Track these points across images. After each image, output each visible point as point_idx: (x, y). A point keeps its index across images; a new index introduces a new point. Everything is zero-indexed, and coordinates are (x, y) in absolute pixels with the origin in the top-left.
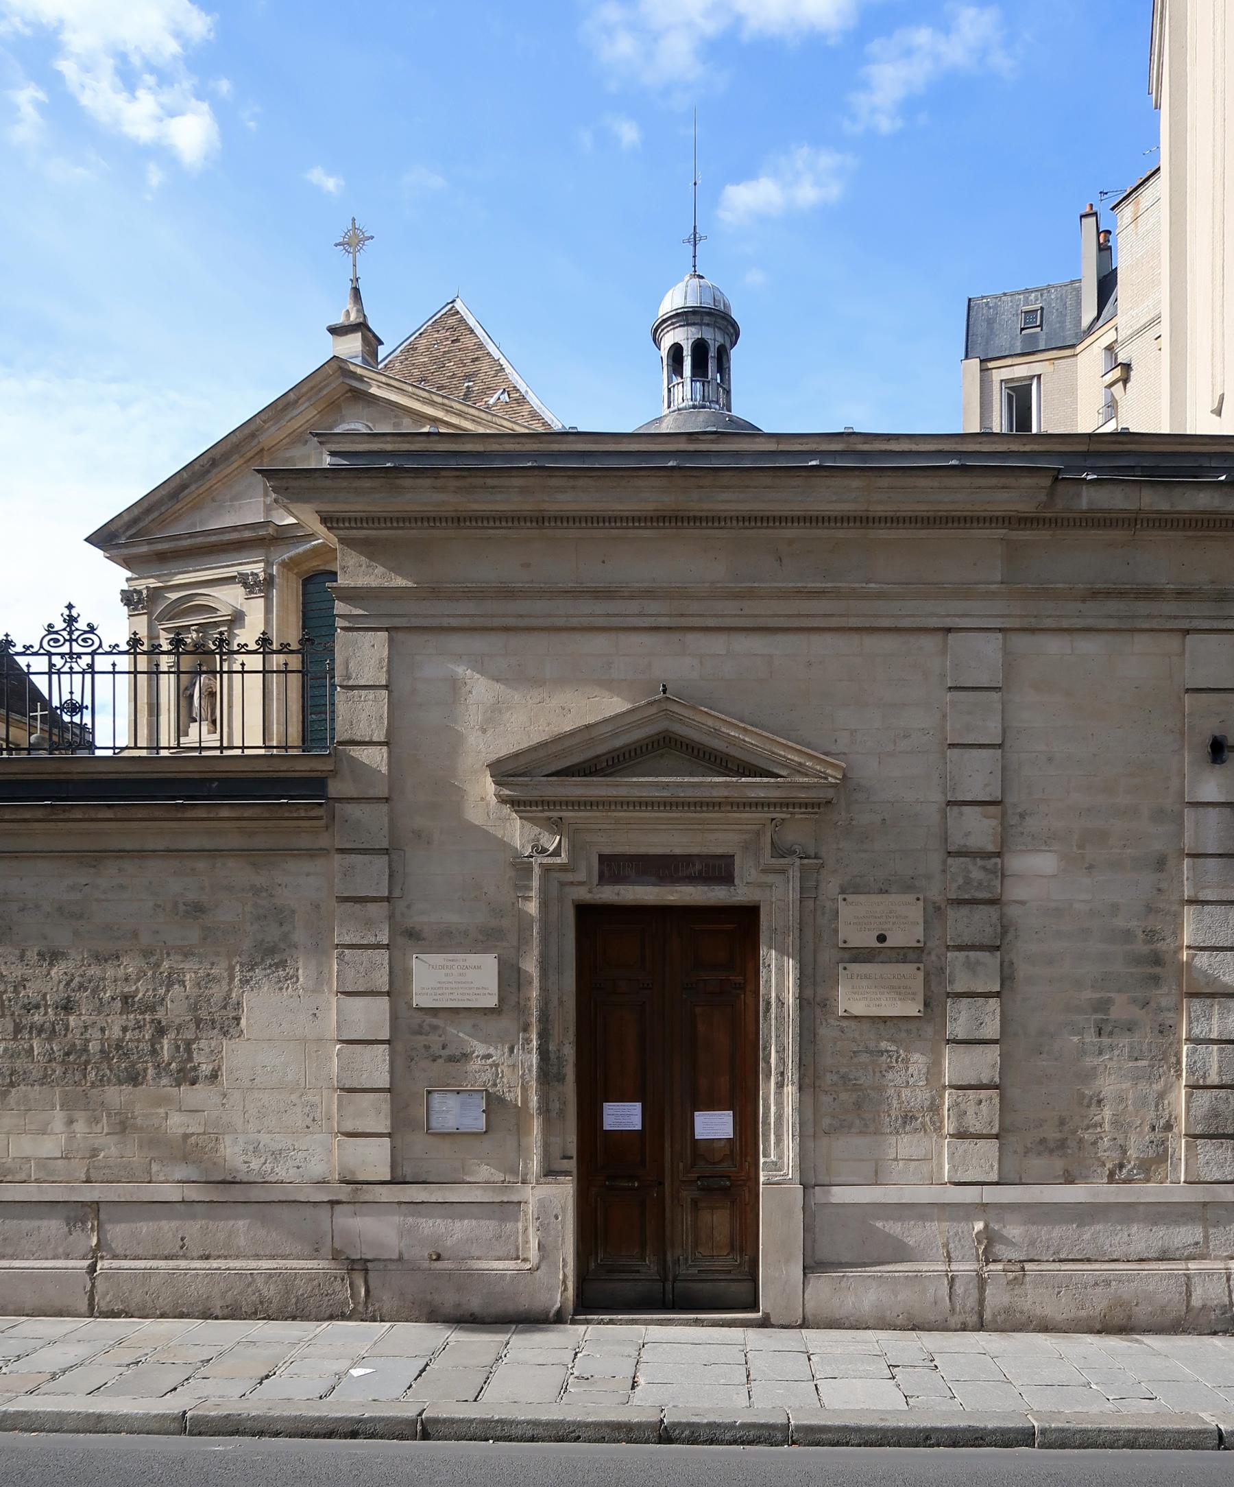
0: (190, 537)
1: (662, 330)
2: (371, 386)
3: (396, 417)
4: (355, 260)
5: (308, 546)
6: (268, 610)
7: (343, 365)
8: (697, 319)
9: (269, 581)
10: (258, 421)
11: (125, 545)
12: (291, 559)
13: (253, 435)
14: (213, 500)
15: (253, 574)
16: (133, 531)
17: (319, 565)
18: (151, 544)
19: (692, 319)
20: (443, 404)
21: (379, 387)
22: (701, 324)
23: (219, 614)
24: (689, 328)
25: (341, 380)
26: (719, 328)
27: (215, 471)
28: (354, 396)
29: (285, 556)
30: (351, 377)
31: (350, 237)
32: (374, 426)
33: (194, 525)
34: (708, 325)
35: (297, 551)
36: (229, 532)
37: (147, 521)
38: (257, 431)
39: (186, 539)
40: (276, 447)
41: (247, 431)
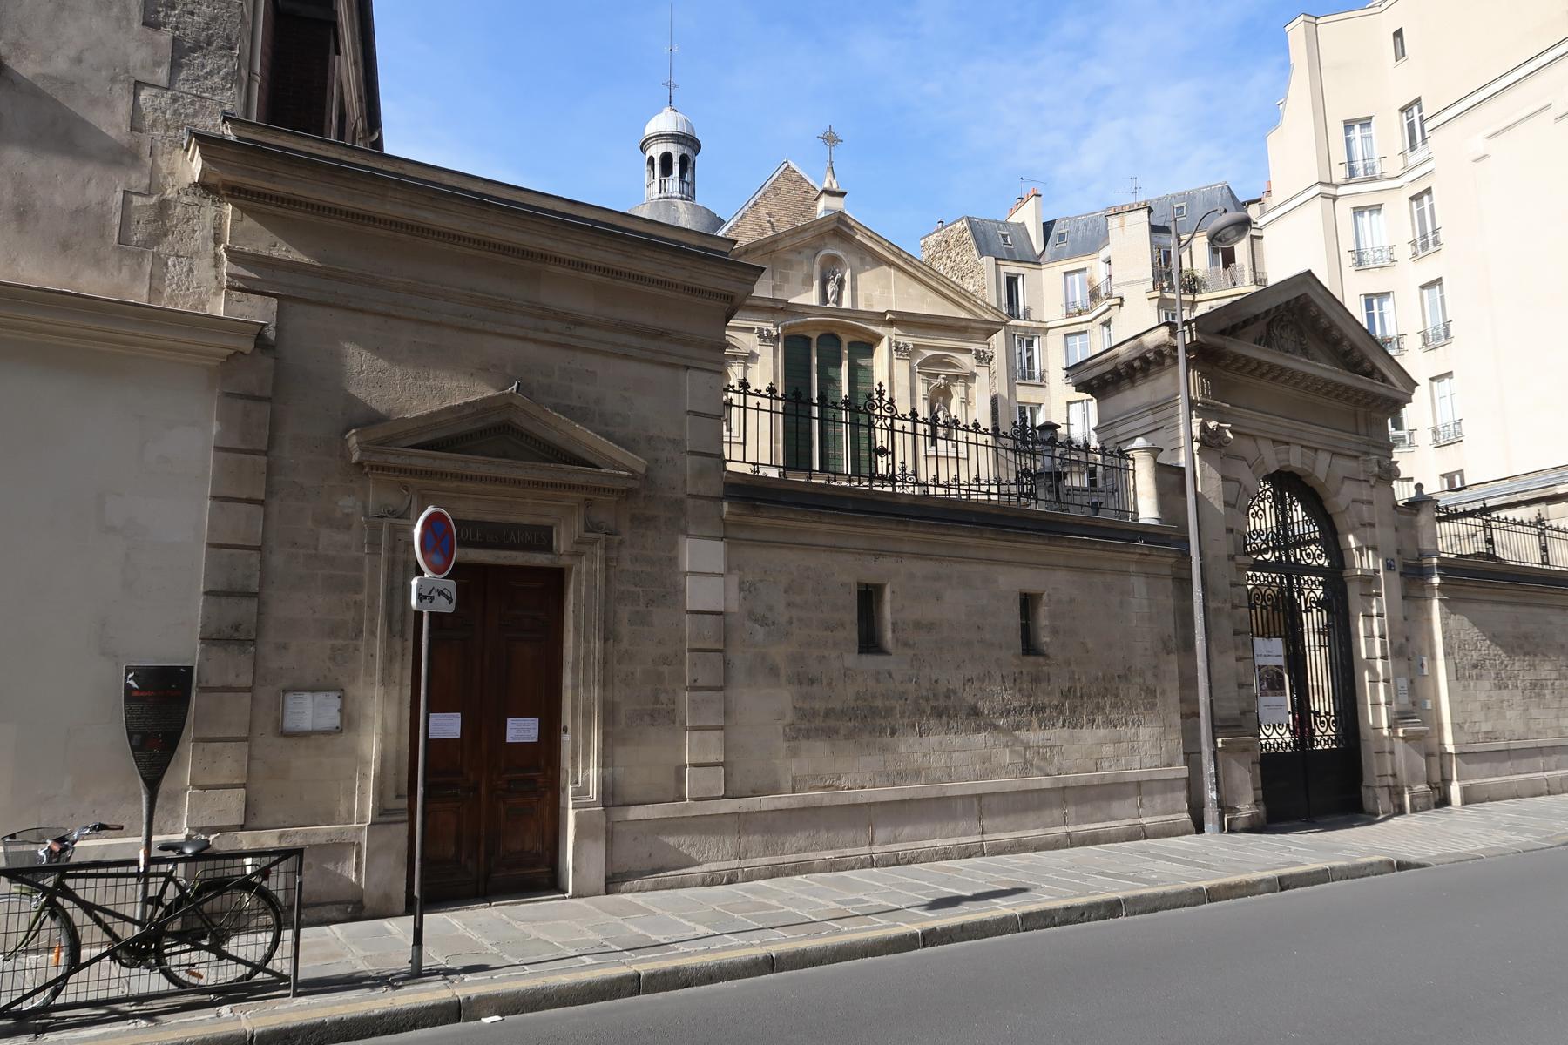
3: (861, 254)
5: (804, 320)
6: (775, 355)
9: (778, 335)
12: (790, 325)
13: (775, 242)
15: (767, 330)
19: (681, 140)
21: (862, 236)
22: (685, 145)
23: (739, 351)
25: (836, 224)
28: (834, 233)
30: (842, 224)
34: (689, 146)
41: (774, 239)
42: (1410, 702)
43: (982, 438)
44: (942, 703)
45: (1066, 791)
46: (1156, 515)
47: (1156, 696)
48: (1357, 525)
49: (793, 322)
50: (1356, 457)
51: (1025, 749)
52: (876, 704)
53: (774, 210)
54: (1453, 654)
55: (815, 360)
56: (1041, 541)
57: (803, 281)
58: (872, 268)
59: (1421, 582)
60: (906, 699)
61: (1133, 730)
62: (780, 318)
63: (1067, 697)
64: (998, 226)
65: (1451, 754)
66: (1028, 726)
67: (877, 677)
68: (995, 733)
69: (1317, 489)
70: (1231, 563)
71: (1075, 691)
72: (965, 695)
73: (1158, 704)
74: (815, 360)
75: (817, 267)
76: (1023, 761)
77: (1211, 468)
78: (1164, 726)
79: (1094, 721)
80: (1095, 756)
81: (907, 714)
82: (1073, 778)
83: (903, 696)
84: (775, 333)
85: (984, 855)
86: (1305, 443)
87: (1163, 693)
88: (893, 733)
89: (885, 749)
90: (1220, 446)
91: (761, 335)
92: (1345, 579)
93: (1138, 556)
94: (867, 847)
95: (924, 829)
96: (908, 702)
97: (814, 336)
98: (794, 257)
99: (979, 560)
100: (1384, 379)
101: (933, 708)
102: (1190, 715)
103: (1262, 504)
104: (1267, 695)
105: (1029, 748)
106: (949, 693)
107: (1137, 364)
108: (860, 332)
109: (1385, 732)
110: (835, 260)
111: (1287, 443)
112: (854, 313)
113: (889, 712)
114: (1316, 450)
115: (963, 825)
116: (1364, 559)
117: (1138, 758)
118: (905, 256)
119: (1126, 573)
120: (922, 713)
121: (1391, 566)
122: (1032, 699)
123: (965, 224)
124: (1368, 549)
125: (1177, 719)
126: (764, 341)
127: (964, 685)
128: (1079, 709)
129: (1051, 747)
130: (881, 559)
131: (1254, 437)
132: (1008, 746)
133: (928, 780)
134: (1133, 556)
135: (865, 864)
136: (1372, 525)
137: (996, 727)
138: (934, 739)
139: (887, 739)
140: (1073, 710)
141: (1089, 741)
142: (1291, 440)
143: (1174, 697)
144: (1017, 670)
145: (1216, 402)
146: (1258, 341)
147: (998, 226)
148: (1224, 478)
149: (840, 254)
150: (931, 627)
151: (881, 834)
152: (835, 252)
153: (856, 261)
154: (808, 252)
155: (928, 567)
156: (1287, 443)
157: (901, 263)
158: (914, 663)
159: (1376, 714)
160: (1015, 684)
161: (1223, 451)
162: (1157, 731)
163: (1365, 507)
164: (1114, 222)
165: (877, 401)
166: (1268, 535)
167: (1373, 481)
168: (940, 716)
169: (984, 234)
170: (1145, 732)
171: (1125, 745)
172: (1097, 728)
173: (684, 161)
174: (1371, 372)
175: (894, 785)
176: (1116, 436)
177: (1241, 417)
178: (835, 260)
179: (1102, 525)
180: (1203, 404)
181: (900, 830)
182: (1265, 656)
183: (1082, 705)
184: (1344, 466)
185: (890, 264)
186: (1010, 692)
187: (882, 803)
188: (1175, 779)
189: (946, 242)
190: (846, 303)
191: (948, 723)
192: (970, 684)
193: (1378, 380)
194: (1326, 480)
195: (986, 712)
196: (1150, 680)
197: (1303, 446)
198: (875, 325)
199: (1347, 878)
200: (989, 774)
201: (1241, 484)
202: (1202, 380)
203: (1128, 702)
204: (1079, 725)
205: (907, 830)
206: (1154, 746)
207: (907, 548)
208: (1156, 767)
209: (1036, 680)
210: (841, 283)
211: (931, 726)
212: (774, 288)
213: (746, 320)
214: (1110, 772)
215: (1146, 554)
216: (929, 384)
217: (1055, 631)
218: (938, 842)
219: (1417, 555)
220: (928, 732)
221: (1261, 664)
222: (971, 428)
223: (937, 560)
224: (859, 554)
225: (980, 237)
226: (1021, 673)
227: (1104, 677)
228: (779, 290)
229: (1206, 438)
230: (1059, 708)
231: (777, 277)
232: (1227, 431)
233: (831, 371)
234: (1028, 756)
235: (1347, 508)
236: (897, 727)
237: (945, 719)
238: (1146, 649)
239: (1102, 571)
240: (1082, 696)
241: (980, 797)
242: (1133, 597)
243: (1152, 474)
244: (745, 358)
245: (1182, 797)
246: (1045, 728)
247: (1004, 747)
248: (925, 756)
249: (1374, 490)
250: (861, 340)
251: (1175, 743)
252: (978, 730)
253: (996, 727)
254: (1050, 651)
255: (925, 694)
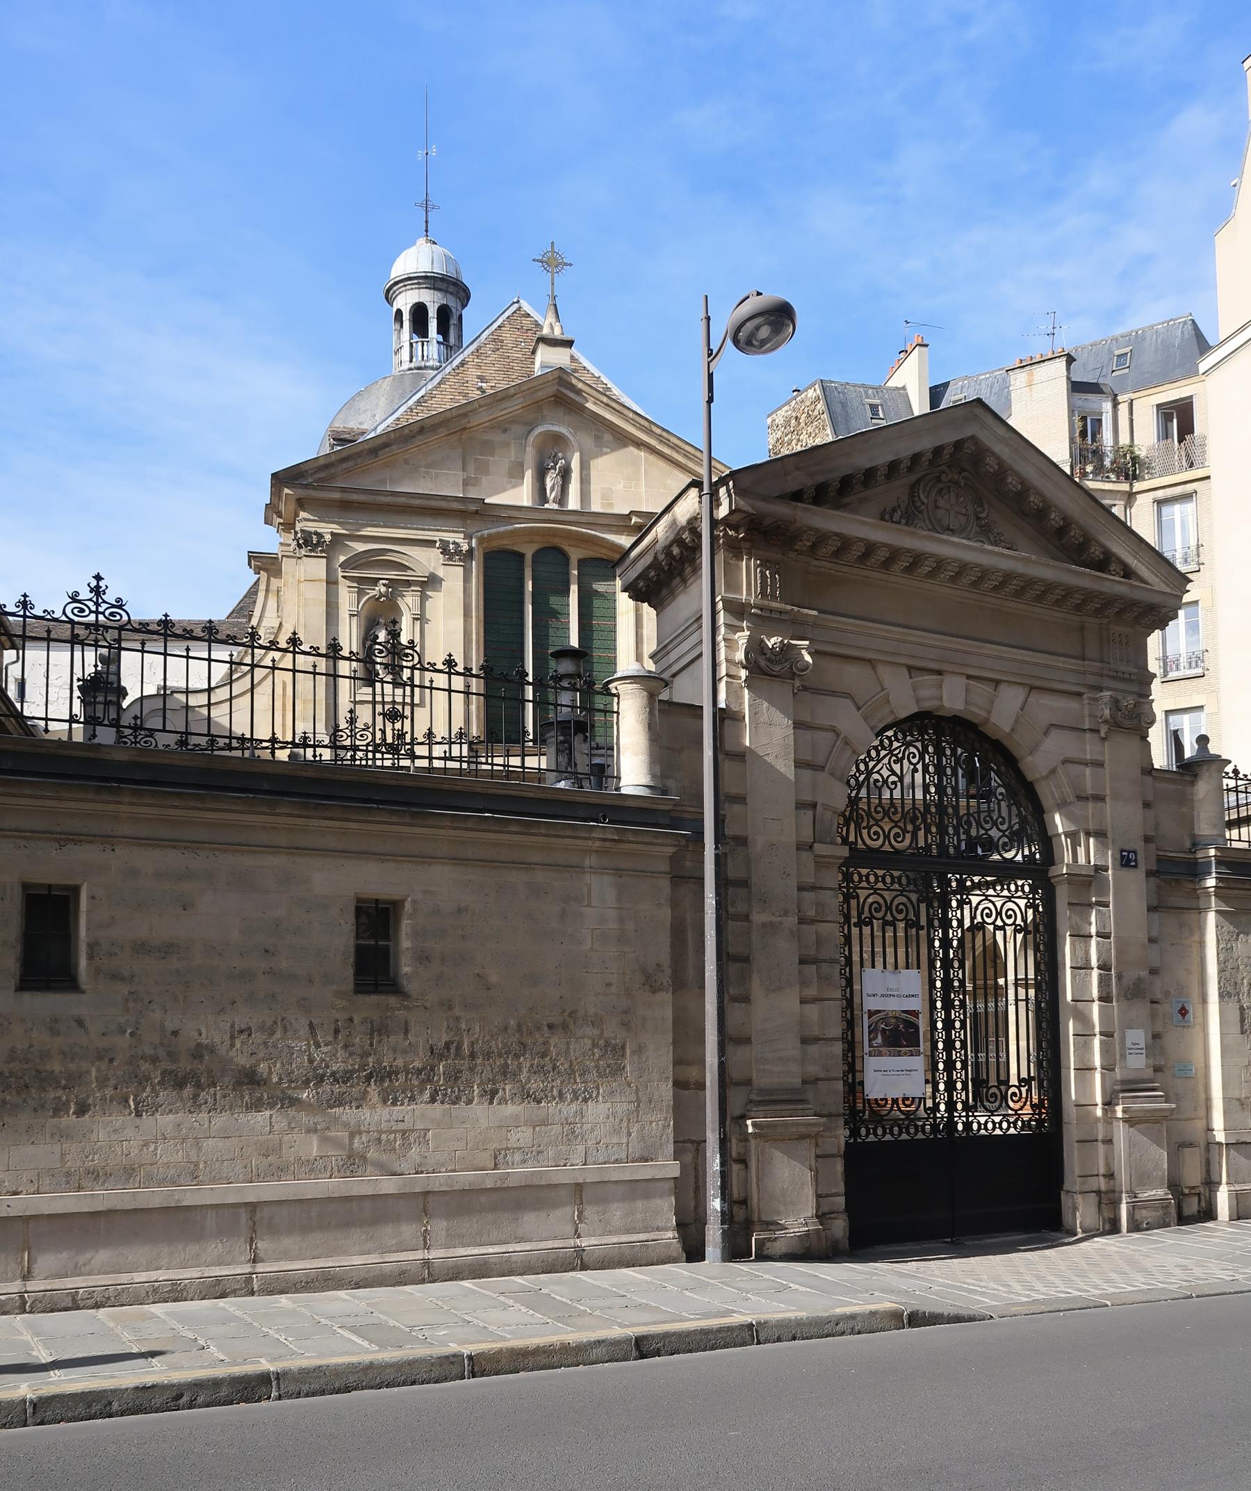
0: (391, 495)
1: (405, 286)
2: (587, 401)
3: (597, 430)
4: (553, 280)
5: (510, 527)
6: (467, 580)
7: (565, 377)
8: (444, 286)
9: (471, 551)
10: (476, 403)
11: (306, 486)
12: (490, 535)
13: (465, 415)
14: (406, 462)
15: (454, 543)
16: (322, 475)
17: (507, 545)
18: (346, 492)
19: (439, 284)
20: (660, 436)
21: (595, 403)
22: (446, 291)
23: (413, 573)
24: (436, 292)
25: (556, 387)
26: (459, 298)
27: (419, 437)
29: (486, 532)
30: (567, 388)
31: (549, 258)
32: (575, 433)
33: (383, 482)
34: (451, 293)
35: (498, 530)
36: (436, 500)
37: (339, 468)
38: (471, 412)
39: (387, 496)
40: (476, 428)
41: (461, 411)
42: (1147, 1066)
43: (303, 662)
44: (185, 1065)
45: (430, 1198)
46: (645, 780)
47: (623, 1055)
48: (1072, 798)
49: (493, 531)
50: (1080, 695)
51: (352, 1135)
52: (48, 1067)
53: (489, 372)
54: (1238, 994)
55: (529, 586)
56: (394, 819)
57: (509, 473)
58: (613, 451)
59: (1191, 886)
60: (111, 1060)
61: (574, 1107)
62: (474, 526)
63: (441, 1057)
64: (866, 393)
65: (1220, 1144)
66: (361, 1100)
67: (53, 1025)
68: (292, 1112)
69: (1005, 742)
70: (805, 855)
71: (459, 1048)
72: (232, 1053)
73: (628, 1068)
74: (529, 586)
75: (529, 450)
76: (344, 1153)
77: (773, 709)
78: (638, 1101)
79: (494, 1093)
80: (496, 1146)
81: (112, 1082)
82: (439, 1180)
83: (106, 1055)
84: (465, 547)
85: (252, 1293)
86: (972, 672)
87: (639, 1050)
88: (82, 1110)
89: (63, 1135)
90: (793, 676)
91: (445, 551)
92: (1052, 881)
93: (597, 844)
94: (19, 1282)
95: (138, 1253)
96: (115, 1064)
97: (529, 551)
98: (496, 437)
99: (274, 849)
100: (1128, 573)
101: (164, 1073)
102: (686, 1087)
103: (897, 768)
104: (880, 1054)
105: (360, 1133)
106: (198, 1052)
107: (676, 551)
108: (595, 544)
109: (1099, 1112)
110: (558, 440)
111: (939, 673)
112: (586, 517)
113: (74, 1080)
114: (997, 683)
115: (214, 1248)
116: (1081, 851)
117: (581, 1148)
118: (658, 431)
119: (579, 868)
120: (143, 1081)
121: (1129, 860)
122: (371, 1059)
123: (818, 392)
124: (1088, 834)
125: (666, 1091)
126: (450, 559)
127: (232, 1037)
128: (465, 1075)
129: (404, 1132)
130: (70, 846)
131: (869, 661)
132: (316, 1131)
133: (150, 1180)
134: (590, 843)
135: (7, 1308)
136: (1099, 798)
137: (294, 1102)
138: (165, 1121)
139: (69, 1120)
140: (454, 1077)
141: (484, 1124)
142: (944, 667)
143: (660, 1056)
144: (342, 1016)
145: (789, 607)
146: (886, 516)
147: (866, 393)
148: (798, 725)
149: (563, 430)
150: (168, 949)
151: (46, 1261)
152: (556, 428)
153: (588, 441)
154: (517, 429)
155: (173, 859)
156: (939, 673)
157: (653, 442)
158: (131, 1005)
159: (1084, 1085)
160: (336, 1037)
161: (797, 683)
162: (622, 1108)
163: (1088, 771)
164: (1018, 379)
165: (90, 604)
166: (904, 816)
167: (1104, 730)
168: (180, 1084)
169: (844, 405)
170: (597, 1110)
171: (556, 1129)
172: (500, 1103)
173: (444, 313)
174: (1104, 563)
175: (80, 1188)
176: (670, 666)
177: (843, 631)
178: (558, 439)
179: (531, 795)
180: (761, 610)
181: (88, 1256)
182: (882, 996)
183: (471, 1069)
184: (1049, 707)
185: (639, 444)
186: (325, 1049)
187: (51, 1217)
188: (653, 1180)
189: (797, 418)
190: (573, 503)
191: (196, 1096)
192: (244, 1036)
193: (1117, 574)
194: (1013, 730)
195: (275, 1080)
196: (612, 1030)
197: (969, 677)
198: (617, 532)
199: (794, 1338)
200: (280, 1171)
201: (838, 735)
202: (763, 576)
203: (566, 1066)
204: (464, 1099)
205: (102, 1256)
206: (616, 1131)
207: (126, 830)
208: (616, 1161)
209: (379, 1030)
210: (565, 474)
211: (161, 1099)
212: (466, 483)
213: (424, 530)
214: (519, 1171)
215: (612, 840)
216: (361, 593)
217: (423, 958)
218: (161, 1275)
219: (1188, 845)
220: (155, 1108)
221: (873, 1008)
222: (283, 645)
223: (185, 848)
224: (25, 838)
225: (838, 408)
226: (351, 1020)
227: (519, 1026)
228: (474, 485)
229: (763, 663)
230: (427, 1075)
231: (471, 467)
232: (804, 652)
233: (554, 601)
234: (356, 1145)
235: (1053, 771)
236: (90, 1101)
237: (188, 1091)
238: (610, 985)
239: (527, 866)
240: (473, 1056)
241: (253, 1207)
242: (589, 905)
243: (644, 717)
244: (423, 585)
245: (665, 1210)
246: (394, 1104)
247: (308, 1131)
248: (146, 1144)
249: (1107, 745)
250: (599, 556)
251: (660, 1124)
252: (256, 1106)
253: (294, 1102)
254: (411, 987)
255: (149, 1051)
